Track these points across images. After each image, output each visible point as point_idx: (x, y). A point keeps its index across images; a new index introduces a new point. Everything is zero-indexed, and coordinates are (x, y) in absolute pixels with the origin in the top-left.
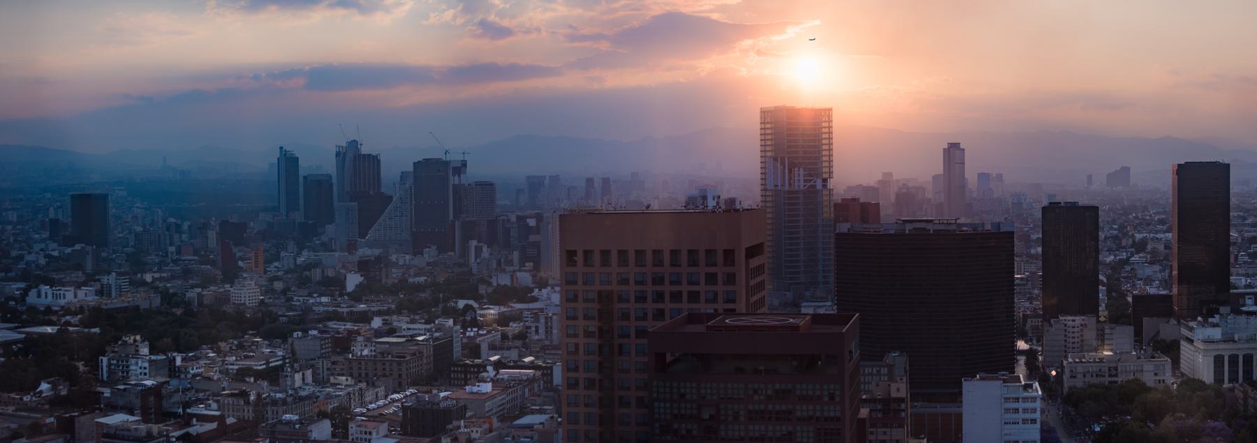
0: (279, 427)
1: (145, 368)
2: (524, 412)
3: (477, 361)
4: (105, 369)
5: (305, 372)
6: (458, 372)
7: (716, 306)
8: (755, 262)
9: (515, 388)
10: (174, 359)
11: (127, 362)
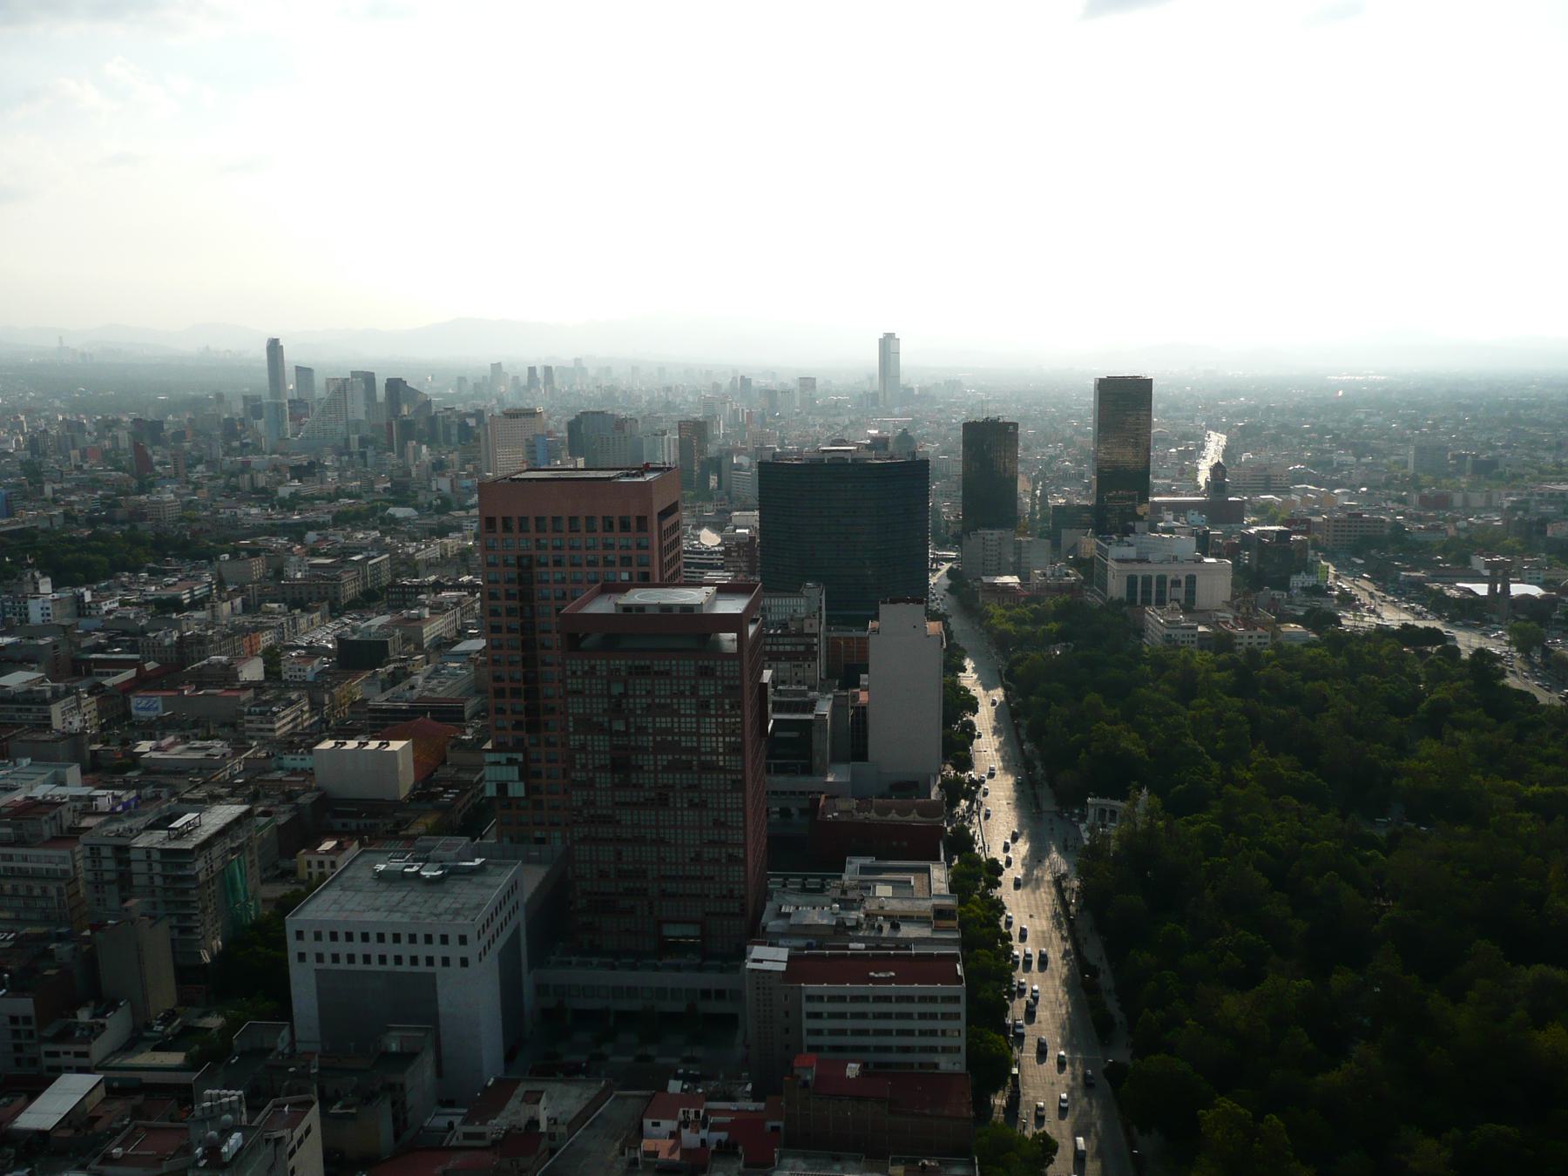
1: (47, 609)
6: (395, 593)
8: (667, 523)
10: (83, 595)
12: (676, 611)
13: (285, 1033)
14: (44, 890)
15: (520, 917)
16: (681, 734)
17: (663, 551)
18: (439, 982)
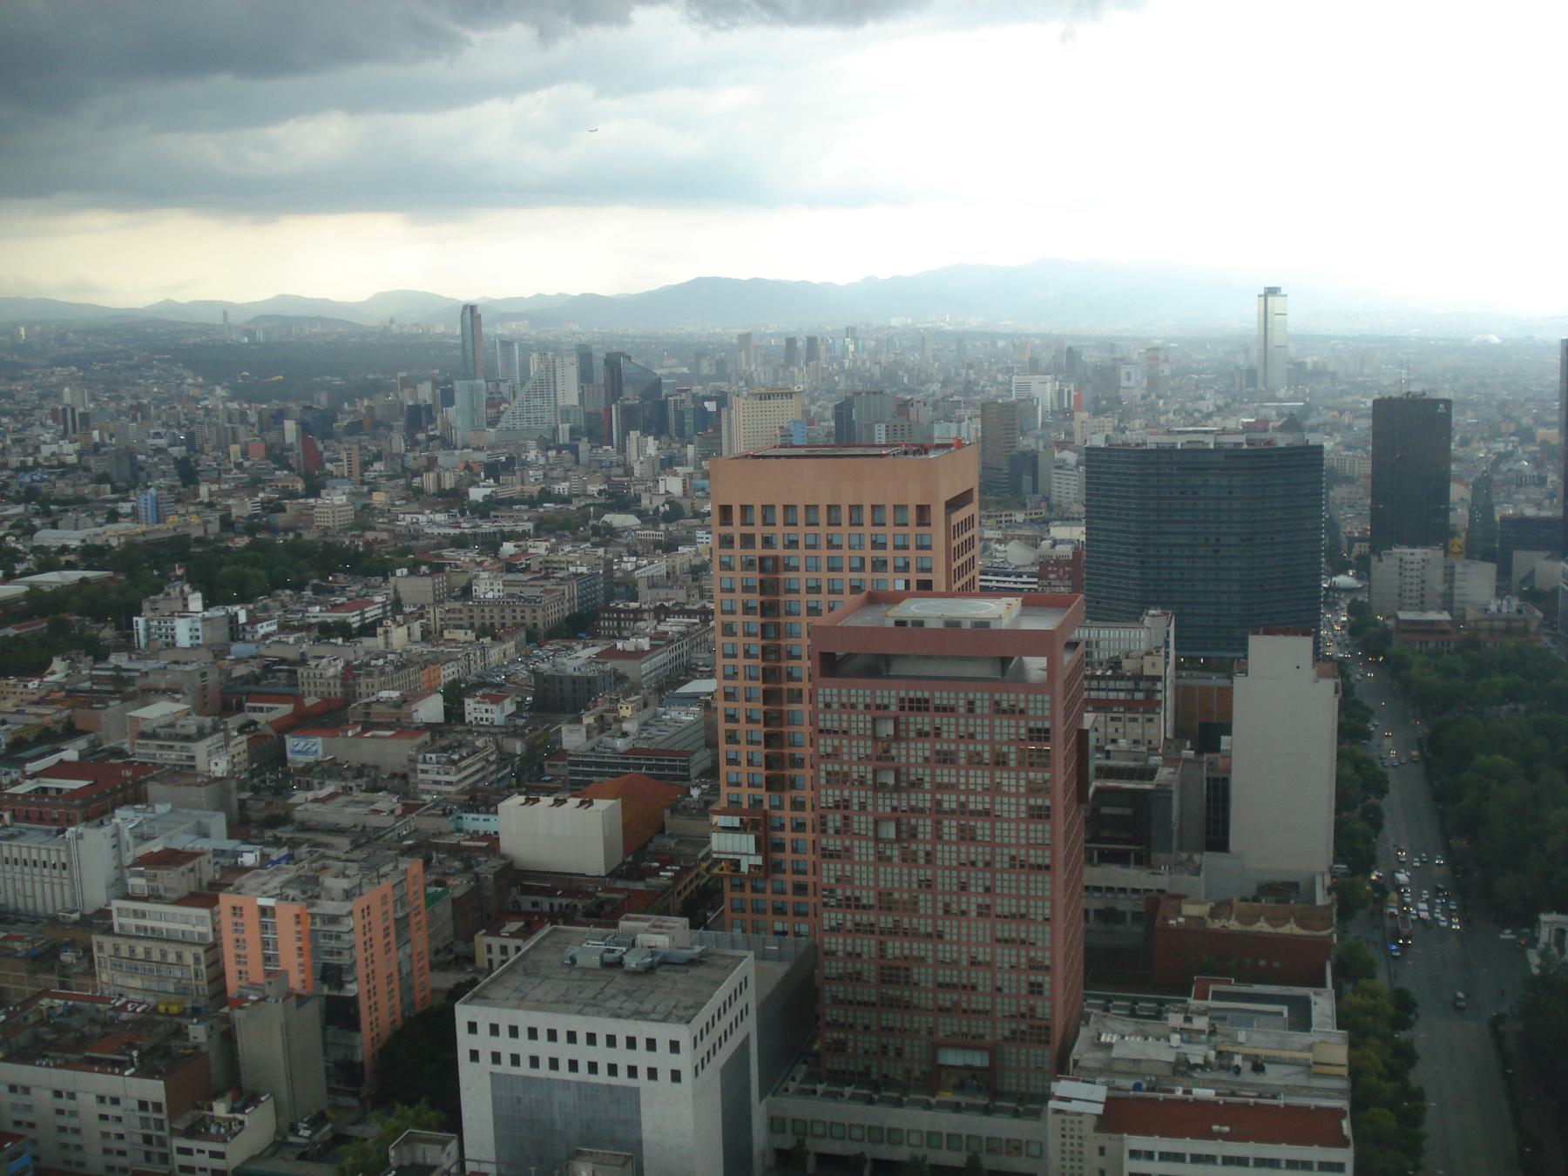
0: (375, 709)
2: (689, 671)
3: (633, 605)
7: (907, 576)
8: (959, 516)
10: (236, 615)
12: (967, 625)
13: (453, 1147)
14: (179, 956)
15: (750, 1025)
16: (968, 792)
17: (953, 553)
18: (643, 1100)
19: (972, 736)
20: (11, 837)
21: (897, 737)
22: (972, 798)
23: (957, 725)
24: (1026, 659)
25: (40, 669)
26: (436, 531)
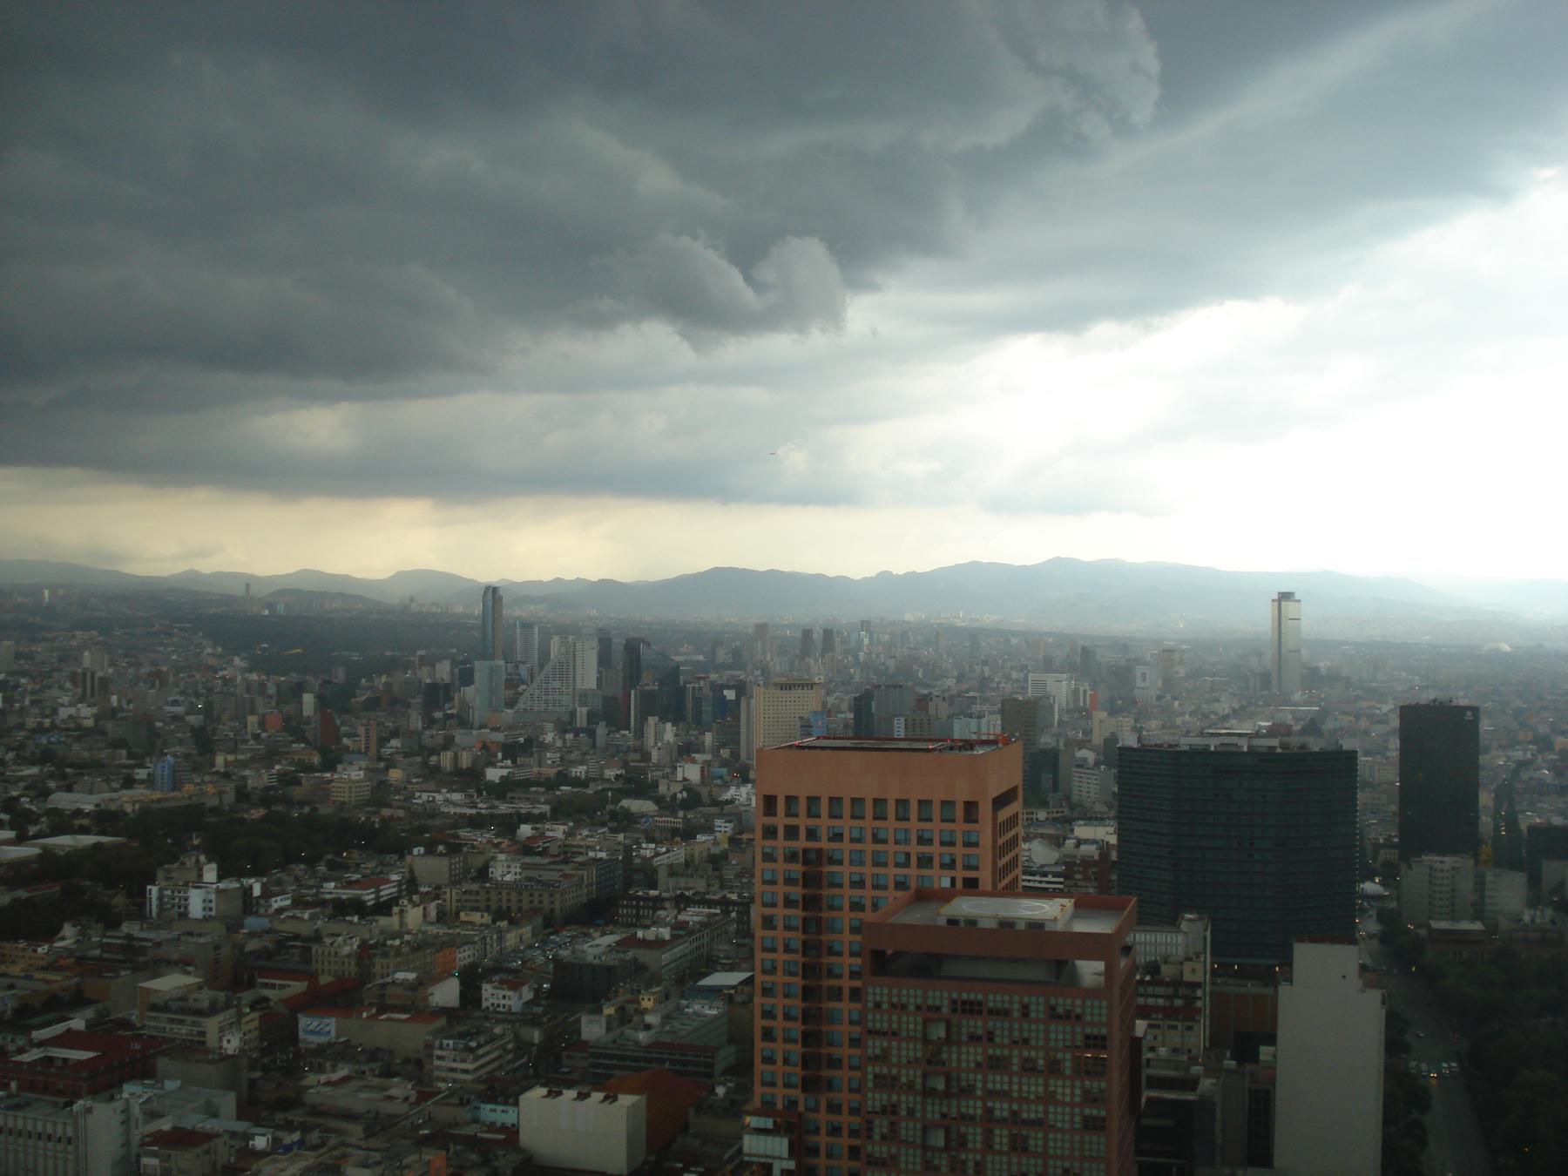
0: (391, 990)
1: (211, 901)
2: (711, 965)
3: (653, 893)
4: (155, 902)
5: (427, 906)
7: (952, 873)
8: (1004, 814)
9: (701, 934)
11: (185, 893)
12: (1021, 926)
16: (1021, 1100)
19: (1026, 1041)
20: (18, 1107)
21: (948, 1041)
22: (1025, 1107)
23: (1011, 1029)
24: (1079, 963)
25: (51, 934)
26: (452, 810)
